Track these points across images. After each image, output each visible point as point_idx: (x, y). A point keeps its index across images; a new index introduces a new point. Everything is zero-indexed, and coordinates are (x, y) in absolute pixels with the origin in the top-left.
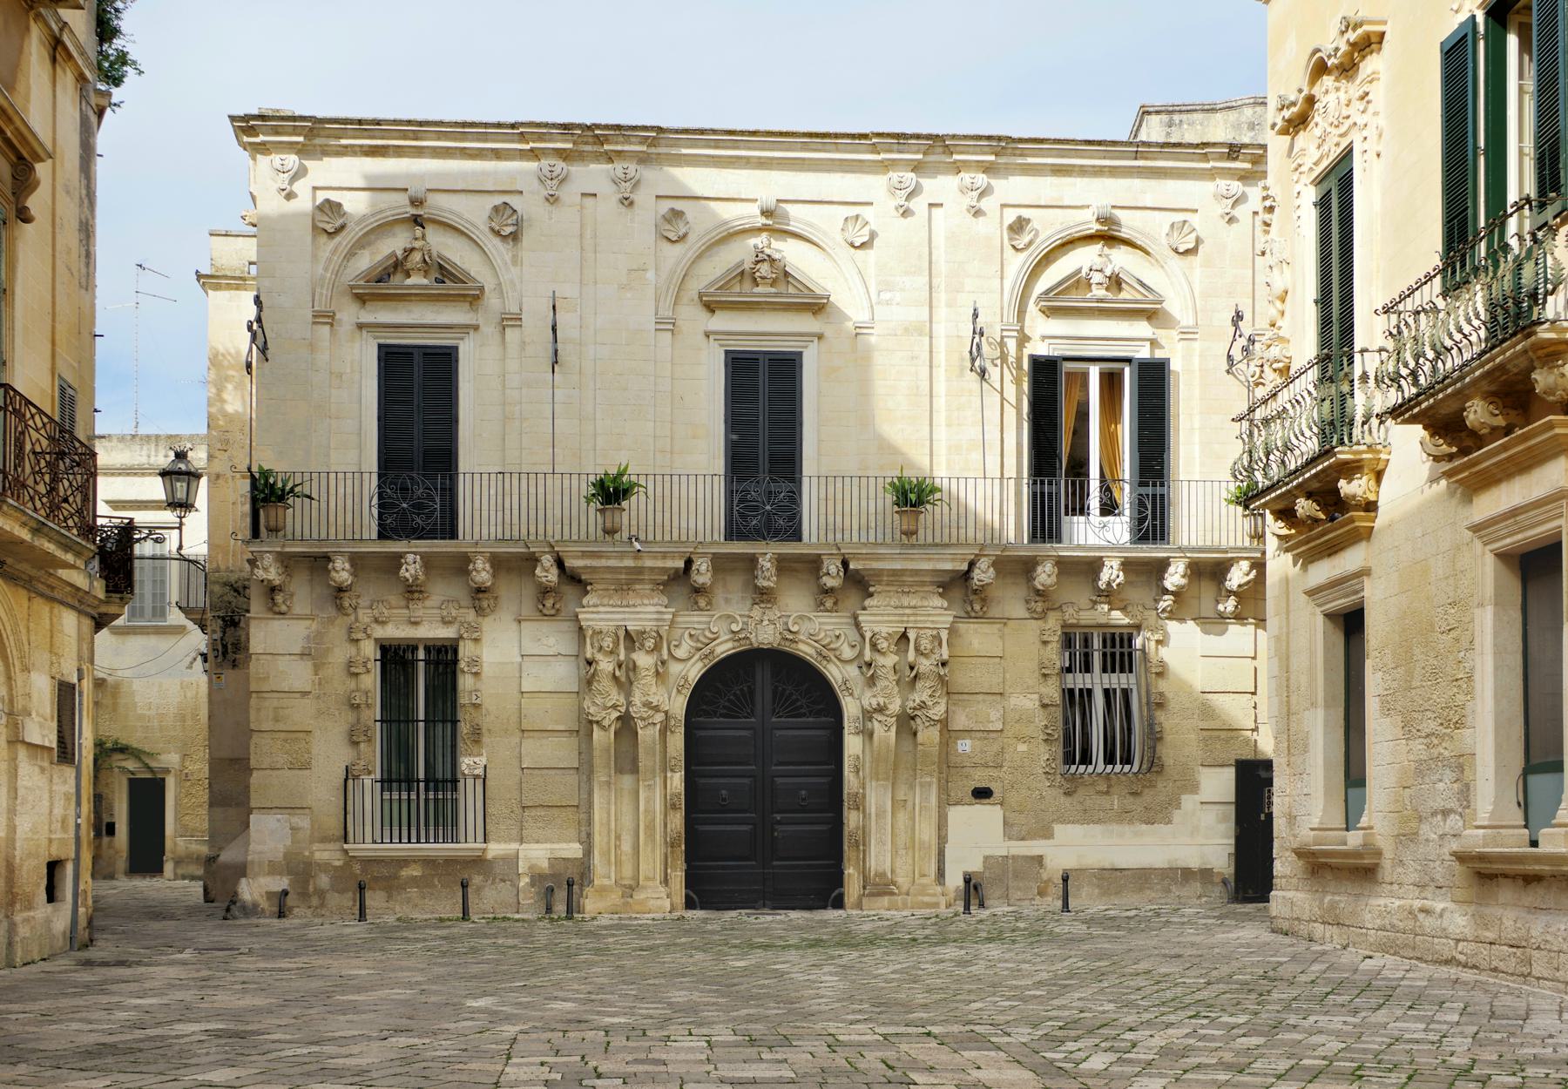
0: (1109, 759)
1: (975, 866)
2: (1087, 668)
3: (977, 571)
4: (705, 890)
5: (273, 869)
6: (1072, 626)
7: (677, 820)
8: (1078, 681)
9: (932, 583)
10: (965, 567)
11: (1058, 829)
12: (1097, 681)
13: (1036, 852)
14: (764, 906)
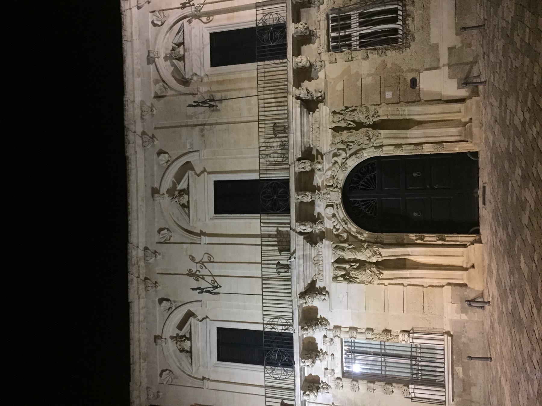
0: (394, 20)
1: (454, 83)
3: (302, 96)
6: (328, 46)
7: (430, 238)
8: (355, 42)
9: (308, 117)
10: (299, 102)
11: (433, 41)
12: (356, 30)
13: (446, 51)
14: (477, 193)
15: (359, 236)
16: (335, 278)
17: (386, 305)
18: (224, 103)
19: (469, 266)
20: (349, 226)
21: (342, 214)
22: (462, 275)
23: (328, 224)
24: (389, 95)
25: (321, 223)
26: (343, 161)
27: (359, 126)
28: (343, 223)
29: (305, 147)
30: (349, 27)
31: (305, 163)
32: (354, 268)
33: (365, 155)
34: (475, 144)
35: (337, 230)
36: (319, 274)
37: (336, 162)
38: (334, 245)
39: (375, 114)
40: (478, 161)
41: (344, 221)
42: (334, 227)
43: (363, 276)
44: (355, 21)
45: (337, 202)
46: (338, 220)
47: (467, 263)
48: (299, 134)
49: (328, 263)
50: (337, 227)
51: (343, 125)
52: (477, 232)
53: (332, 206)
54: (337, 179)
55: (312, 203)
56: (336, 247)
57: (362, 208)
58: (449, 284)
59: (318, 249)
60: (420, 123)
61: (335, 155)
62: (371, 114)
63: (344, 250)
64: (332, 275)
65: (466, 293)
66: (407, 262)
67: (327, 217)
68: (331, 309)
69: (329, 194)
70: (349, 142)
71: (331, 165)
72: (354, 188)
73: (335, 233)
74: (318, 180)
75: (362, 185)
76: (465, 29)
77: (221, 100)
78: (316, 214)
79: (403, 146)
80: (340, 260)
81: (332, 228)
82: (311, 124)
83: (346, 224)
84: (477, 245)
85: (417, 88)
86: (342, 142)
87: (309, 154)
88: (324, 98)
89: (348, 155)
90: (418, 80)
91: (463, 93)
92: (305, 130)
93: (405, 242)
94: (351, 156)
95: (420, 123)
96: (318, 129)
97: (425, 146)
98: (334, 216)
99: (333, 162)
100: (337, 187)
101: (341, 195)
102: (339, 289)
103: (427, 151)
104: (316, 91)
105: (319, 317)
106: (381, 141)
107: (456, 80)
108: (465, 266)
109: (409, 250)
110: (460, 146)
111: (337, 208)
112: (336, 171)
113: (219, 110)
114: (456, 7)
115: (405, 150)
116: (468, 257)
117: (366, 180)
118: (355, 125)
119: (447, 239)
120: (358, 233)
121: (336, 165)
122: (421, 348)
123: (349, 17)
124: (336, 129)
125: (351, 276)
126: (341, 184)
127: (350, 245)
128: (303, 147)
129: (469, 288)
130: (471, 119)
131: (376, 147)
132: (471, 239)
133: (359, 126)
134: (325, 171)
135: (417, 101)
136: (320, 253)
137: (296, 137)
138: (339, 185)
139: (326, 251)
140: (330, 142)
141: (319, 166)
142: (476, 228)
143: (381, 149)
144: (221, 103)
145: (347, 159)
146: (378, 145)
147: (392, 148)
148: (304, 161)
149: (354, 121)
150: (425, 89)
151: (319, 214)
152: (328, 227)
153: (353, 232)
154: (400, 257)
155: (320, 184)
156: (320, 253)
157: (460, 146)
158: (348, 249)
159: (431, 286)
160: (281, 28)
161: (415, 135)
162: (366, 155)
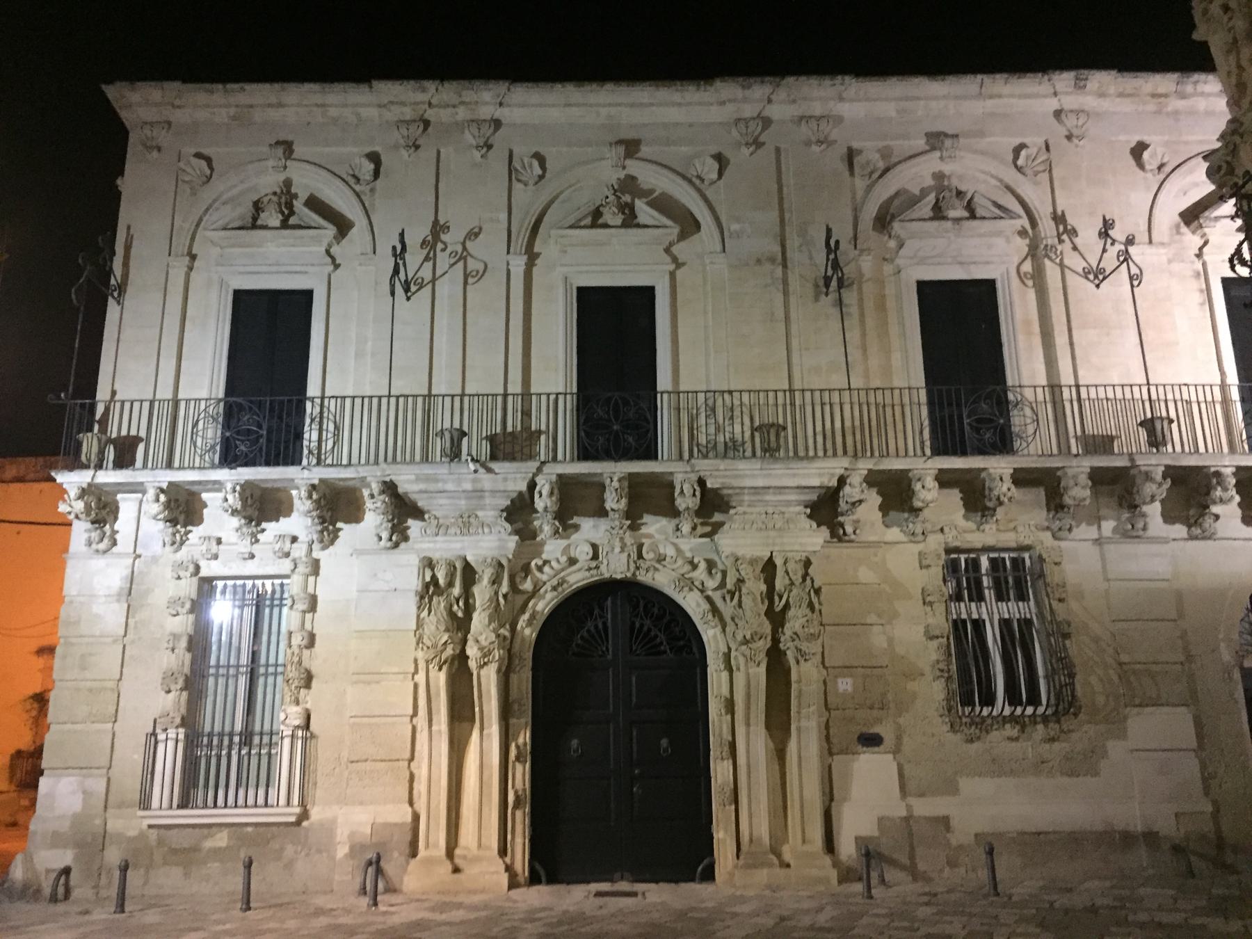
0: (1013, 696)
1: (869, 829)
2: (979, 597)
3: (847, 489)
4: (550, 860)
5: (57, 840)
6: (958, 550)
7: (521, 775)
9: (799, 503)
10: (834, 483)
12: (992, 612)
14: (622, 879)
15: (526, 616)
16: (429, 563)
17: (368, 677)
18: (835, 312)
19: (457, 861)
20: (549, 596)
21: (577, 578)
22: (436, 846)
23: (553, 549)
24: (845, 685)
25: (556, 532)
26: (697, 583)
27: (777, 619)
28: (555, 582)
29: (729, 495)
30: (1001, 597)
31: (694, 495)
32: (451, 606)
33: (711, 632)
34: (731, 875)
35: (540, 569)
36: (439, 526)
37: (694, 567)
38: (504, 562)
39: (802, 655)
40: (692, 880)
41: (559, 584)
42: (546, 562)
43: (435, 625)
44: (1013, 609)
45: (603, 568)
46: (563, 570)
47: (465, 857)
48: (760, 483)
49: (462, 548)
50: (546, 569)
51: (780, 583)
52: (534, 879)
53: (595, 557)
54: (656, 569)
55: (602, 512)
56: (500, 565)
57: (590, 625)
58: (416, 817)
59: (496, 524)
60: (780, 754)
61: (711, 565)
62: (804, 646)
63: (494, 583)
64: (435, 556)
65: (396, 854)
66: (466, 725)
67: (569, 546)
68: (358, 552)
69: (622, 550)
70: (740, 597)
71: (689, 555)
72: (636, 607)
73: (533, 564)
74: (655, 526)
75: (642, 626)
76: (990, 852)
77: (840, 303)
78: (576, 520)
79: (729, 717)
80: (470, 574)
81: (544, 556)
82: (783, 509)
83: (554, 589)
84: (504, 879)
85: (860, 747)
86: (741, 581)
87: (713, 504)
88: (840, 540)
89: (710, 593)
90: (876, 749)
91: (847, 848)
92: (768, 498)
93: (513, 721)
94: (709, 599)
95: (780, 754)
96: (770, 525)
97: (728, 764)
98: (572, 561)
99: (696, 561)
100: (638, 568)
101: (619, 576)
102: (403, 572)
103: (719, 769)
104: (858, 521)
105: (339, 525)
106: (742, 668)
107: (876, 834)
108: (458, 852)
109: (494, 730)
110: (728, 841)
111: (590, 569)
112: (675, 566)
113: (817, 299)
114: (1039, 834)
115: (720, 721)
116: (476, 860)
117: (652, 634)
118: (778, 609)
119: (519, 814)
120: (533, 616)
121: (688, 567)
122: (270, 755)
123: (1022, 597)
124: (769, 568)
125: (435, 599)
126: (643, 577)
127: (505, 596)
128: (730, 492)
129: (408, 863)
130: (788, 866)
131: (727, 657)
132: (518, 866)
133: (777, 619)
134: (676, 541)
135: (830, 748)
136: (486, 530)
137: (753, 476)
138: (643, 572)
139: (490, 544)
140: (740, 554)
141: (686, 528)
142: (544, 879)
143: (722, 667)
144: (834, 306)
145: (702, 591)
146: (733, 662)
147: (725, 691)
148: (698, 493)
149: (787, 606)
150: (856, 765)
151: (576, 527)
152: (547, 548)
153: (535, 605)
154: (477, 709)
155: (644, 530)
156: (486, 530)
157: (728, 841)
158: (496, 593)
159: (412, 778)
160: (1003, 443)
161: (755, 743)
162: (710, 635)
